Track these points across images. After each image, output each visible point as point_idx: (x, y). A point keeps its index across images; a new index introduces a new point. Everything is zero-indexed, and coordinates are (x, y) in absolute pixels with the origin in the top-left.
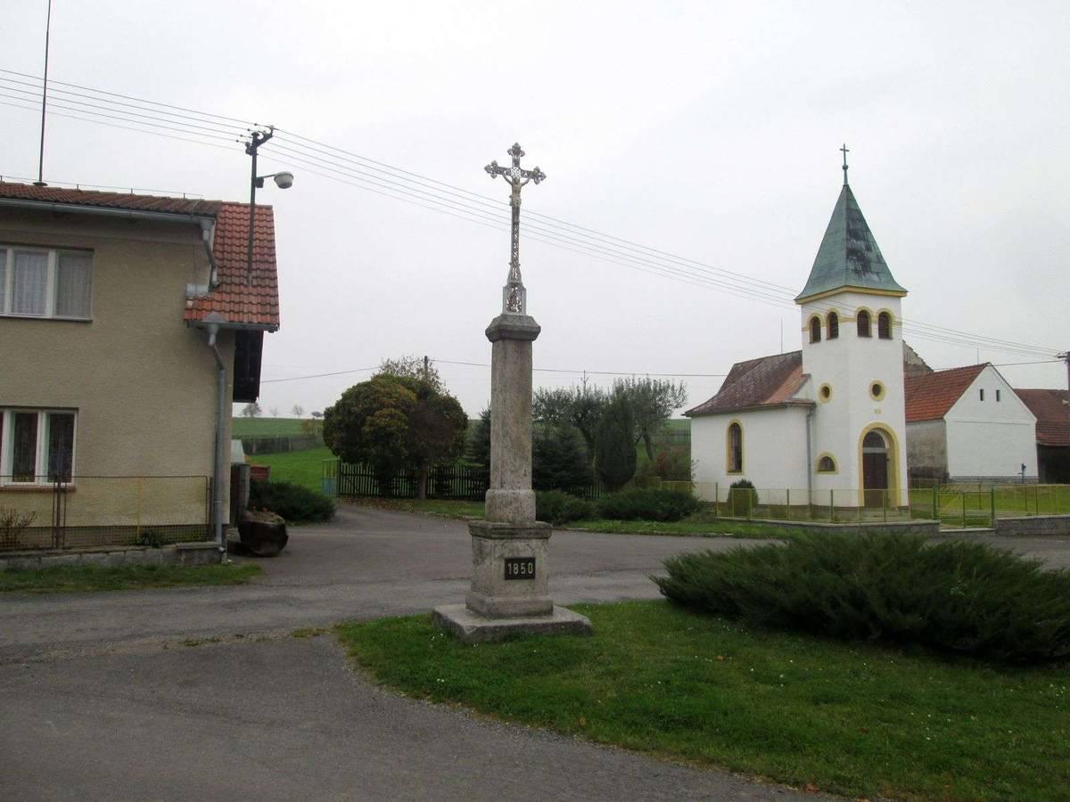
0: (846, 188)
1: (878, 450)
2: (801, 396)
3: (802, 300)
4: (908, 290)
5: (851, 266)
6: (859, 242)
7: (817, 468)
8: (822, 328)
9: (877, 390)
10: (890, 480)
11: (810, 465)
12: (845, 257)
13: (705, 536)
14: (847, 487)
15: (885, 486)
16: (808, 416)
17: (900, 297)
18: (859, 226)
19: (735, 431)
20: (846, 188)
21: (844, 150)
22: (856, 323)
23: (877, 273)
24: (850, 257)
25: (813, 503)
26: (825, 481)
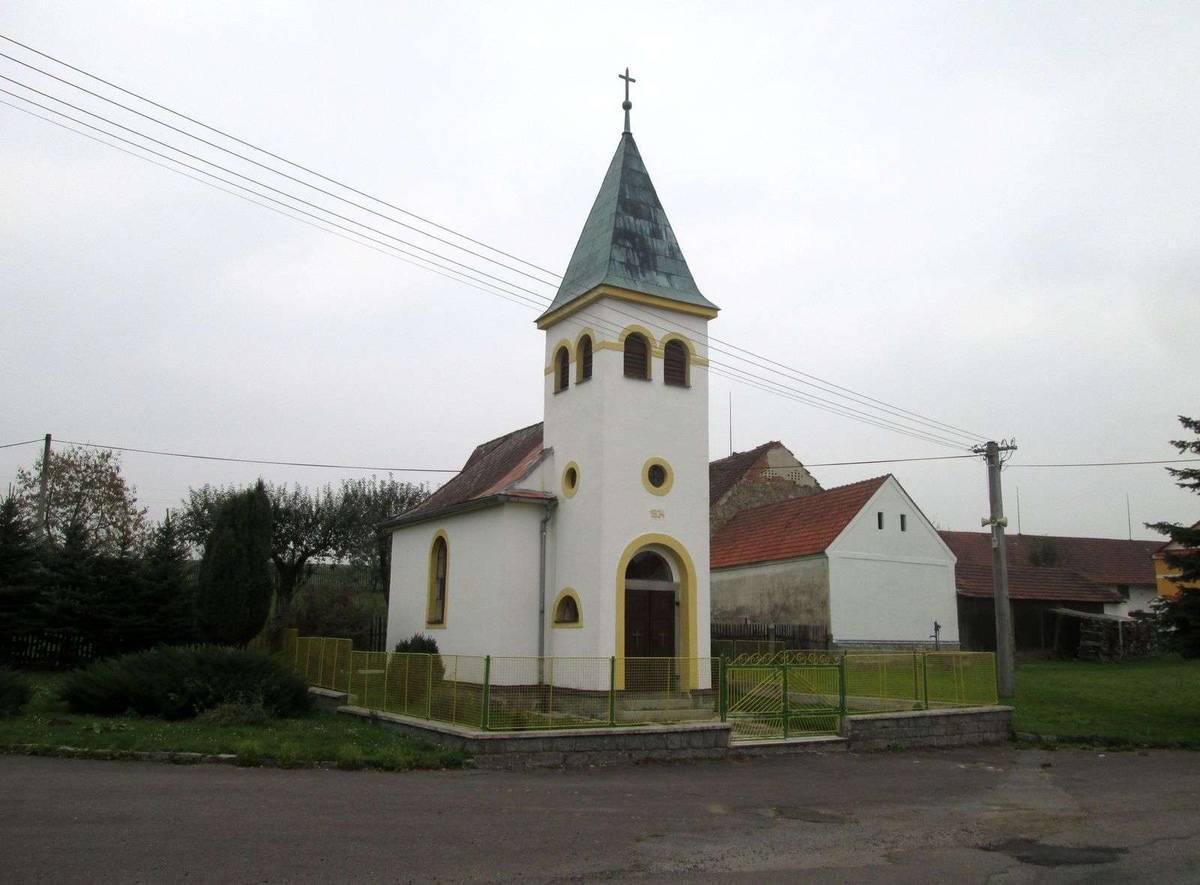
0: (627, 137)
1: (659, 586)
2: (533, 484)
3: (547, 322)
4: (719, 306)
5: (619, 256)
6: (638, 222)
7: (555, 619)
8: (570, 367)
9: (657, 475)
10: (679, 644)
11: (542, 612)
12: (610, 241)
13: (174, 761)
14: (594, 652)
15: (670, 650)
16: (544, 522)
17: (709, 318)
18: (643, 197)
19: (440, 547)
20: (627, 137)
21: (627, 78)
22: (621, 355)
23: (669, 275)
24: (620, 241)
25: (546, 681)
26: (565, 638)
